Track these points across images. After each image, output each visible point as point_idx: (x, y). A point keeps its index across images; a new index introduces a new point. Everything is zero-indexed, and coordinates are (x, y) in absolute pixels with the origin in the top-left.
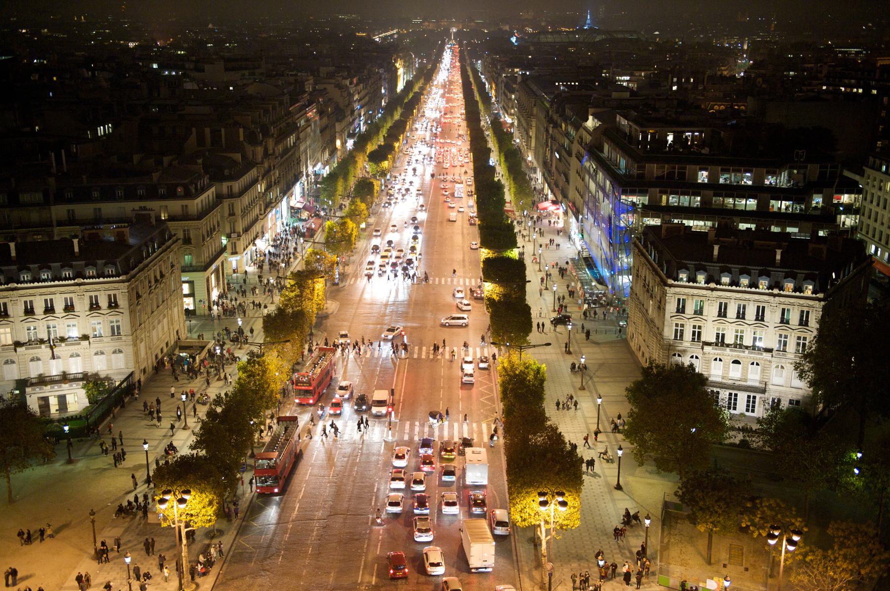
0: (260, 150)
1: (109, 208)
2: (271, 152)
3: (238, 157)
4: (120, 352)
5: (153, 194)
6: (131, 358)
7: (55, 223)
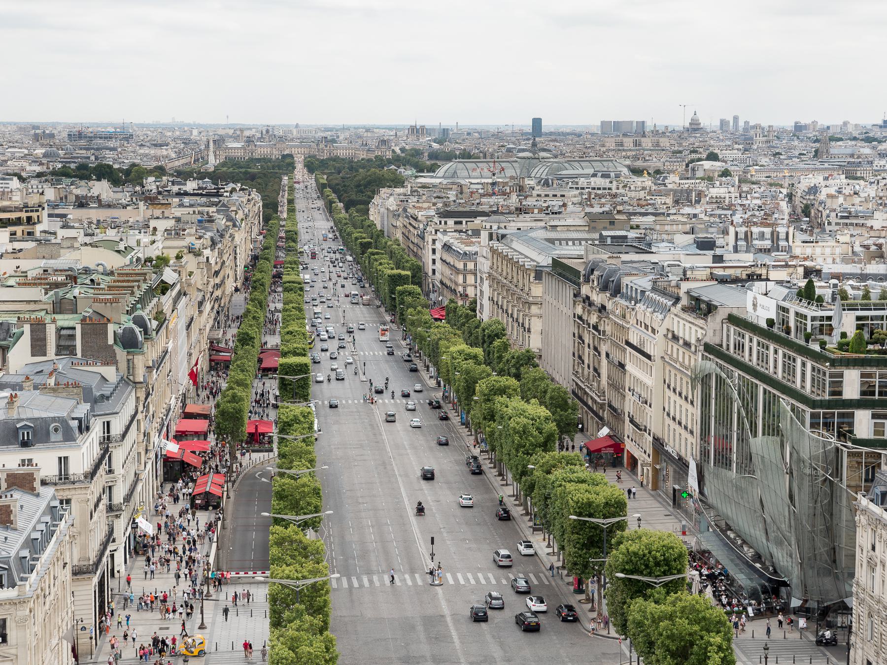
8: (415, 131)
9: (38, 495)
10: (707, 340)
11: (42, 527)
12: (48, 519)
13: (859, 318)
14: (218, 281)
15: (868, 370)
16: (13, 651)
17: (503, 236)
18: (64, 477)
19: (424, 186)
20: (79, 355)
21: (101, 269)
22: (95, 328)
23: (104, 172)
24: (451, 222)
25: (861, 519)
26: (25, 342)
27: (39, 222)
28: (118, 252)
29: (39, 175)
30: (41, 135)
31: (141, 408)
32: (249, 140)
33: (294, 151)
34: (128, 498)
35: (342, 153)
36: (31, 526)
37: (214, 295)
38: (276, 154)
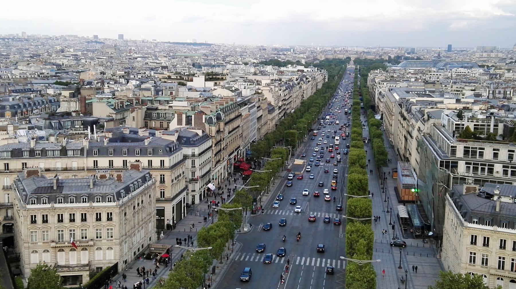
0: (214, 129)
1: (118, 162)
2: (222, 130)
3: (200, 133)
4: (112, 249)
5: (143, 152)
6: (118, 254)
7: (86, 169)
9: (141, 172)
10: (424, 131)
11: (136, 183)
12: (140, 180)
13: (475, 125)
14: (286, 102)
16: (114, 224)
17: (392, 90)
19: (394, 70)
20: (193, 126)
21: (220, 96)
25: (447, 202)
26: (175, 121)
27: (226, 79)
28: (231, 91)
29: (254, 63)
31: (214, 145)
32: (335, 52)
33: (352, 56)
35: (369, 57)
36: (132, 181)
37: (282, 108)
38: (345, 57)
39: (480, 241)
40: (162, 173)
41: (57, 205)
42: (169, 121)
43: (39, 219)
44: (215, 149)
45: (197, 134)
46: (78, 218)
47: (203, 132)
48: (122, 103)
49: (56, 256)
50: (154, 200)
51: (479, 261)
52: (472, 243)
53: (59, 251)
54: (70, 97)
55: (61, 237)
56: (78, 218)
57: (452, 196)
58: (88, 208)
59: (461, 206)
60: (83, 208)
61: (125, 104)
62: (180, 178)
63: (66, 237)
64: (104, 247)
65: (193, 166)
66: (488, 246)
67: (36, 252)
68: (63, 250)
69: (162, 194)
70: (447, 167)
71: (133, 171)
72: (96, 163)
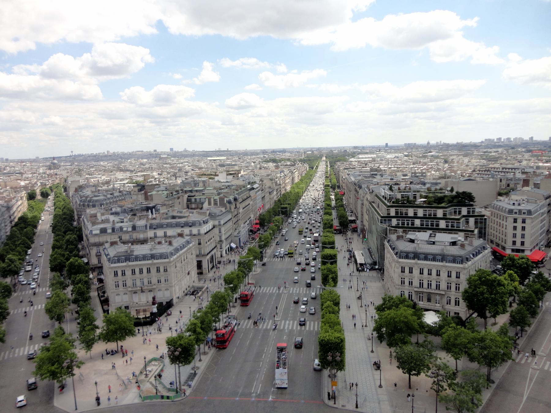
8: (355, 148)
15: (397, 208)
18: (199, 234)
22: (222, 200)
23: (274, 161)
24: (346, 170)
30: (264, 152)
34: (226, 239)
39: (407, 270)
40: (199, 237)
41: (131, 263)
42: (203, 203)
43: (120, 273)
44: (234, 220)
45: (222, 211)
46: (145, 271)
47: (226, 209)
48: (172, 193)
49: (132, 297)
50: (194, 256)
51: (407, 283)
52: (402, 272)
53: (134, 293)
54: (139, 191)
55: (134, 285)
56: (145, 271)
57: (389, 241)
58: (151, 264)
59: (394, 248)
60: (148, 264)
61: (175, 193)
62: (211, 241)
63: (138, 283)
64: (163, 289)
65: (220, 232)
66: (412, 272)
67: (119, 295)
68: (136, 293)
69: (200, 251)
70: (385, 223)
71: (179, 239)
72: (155, 234)
